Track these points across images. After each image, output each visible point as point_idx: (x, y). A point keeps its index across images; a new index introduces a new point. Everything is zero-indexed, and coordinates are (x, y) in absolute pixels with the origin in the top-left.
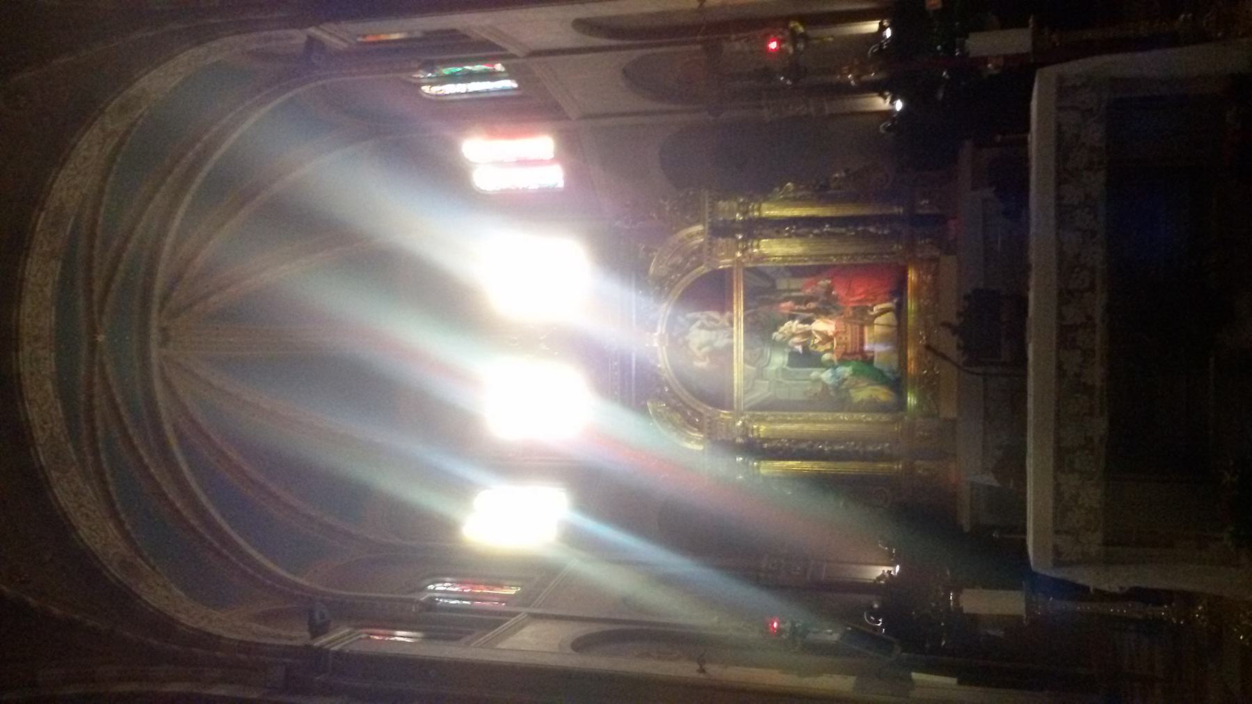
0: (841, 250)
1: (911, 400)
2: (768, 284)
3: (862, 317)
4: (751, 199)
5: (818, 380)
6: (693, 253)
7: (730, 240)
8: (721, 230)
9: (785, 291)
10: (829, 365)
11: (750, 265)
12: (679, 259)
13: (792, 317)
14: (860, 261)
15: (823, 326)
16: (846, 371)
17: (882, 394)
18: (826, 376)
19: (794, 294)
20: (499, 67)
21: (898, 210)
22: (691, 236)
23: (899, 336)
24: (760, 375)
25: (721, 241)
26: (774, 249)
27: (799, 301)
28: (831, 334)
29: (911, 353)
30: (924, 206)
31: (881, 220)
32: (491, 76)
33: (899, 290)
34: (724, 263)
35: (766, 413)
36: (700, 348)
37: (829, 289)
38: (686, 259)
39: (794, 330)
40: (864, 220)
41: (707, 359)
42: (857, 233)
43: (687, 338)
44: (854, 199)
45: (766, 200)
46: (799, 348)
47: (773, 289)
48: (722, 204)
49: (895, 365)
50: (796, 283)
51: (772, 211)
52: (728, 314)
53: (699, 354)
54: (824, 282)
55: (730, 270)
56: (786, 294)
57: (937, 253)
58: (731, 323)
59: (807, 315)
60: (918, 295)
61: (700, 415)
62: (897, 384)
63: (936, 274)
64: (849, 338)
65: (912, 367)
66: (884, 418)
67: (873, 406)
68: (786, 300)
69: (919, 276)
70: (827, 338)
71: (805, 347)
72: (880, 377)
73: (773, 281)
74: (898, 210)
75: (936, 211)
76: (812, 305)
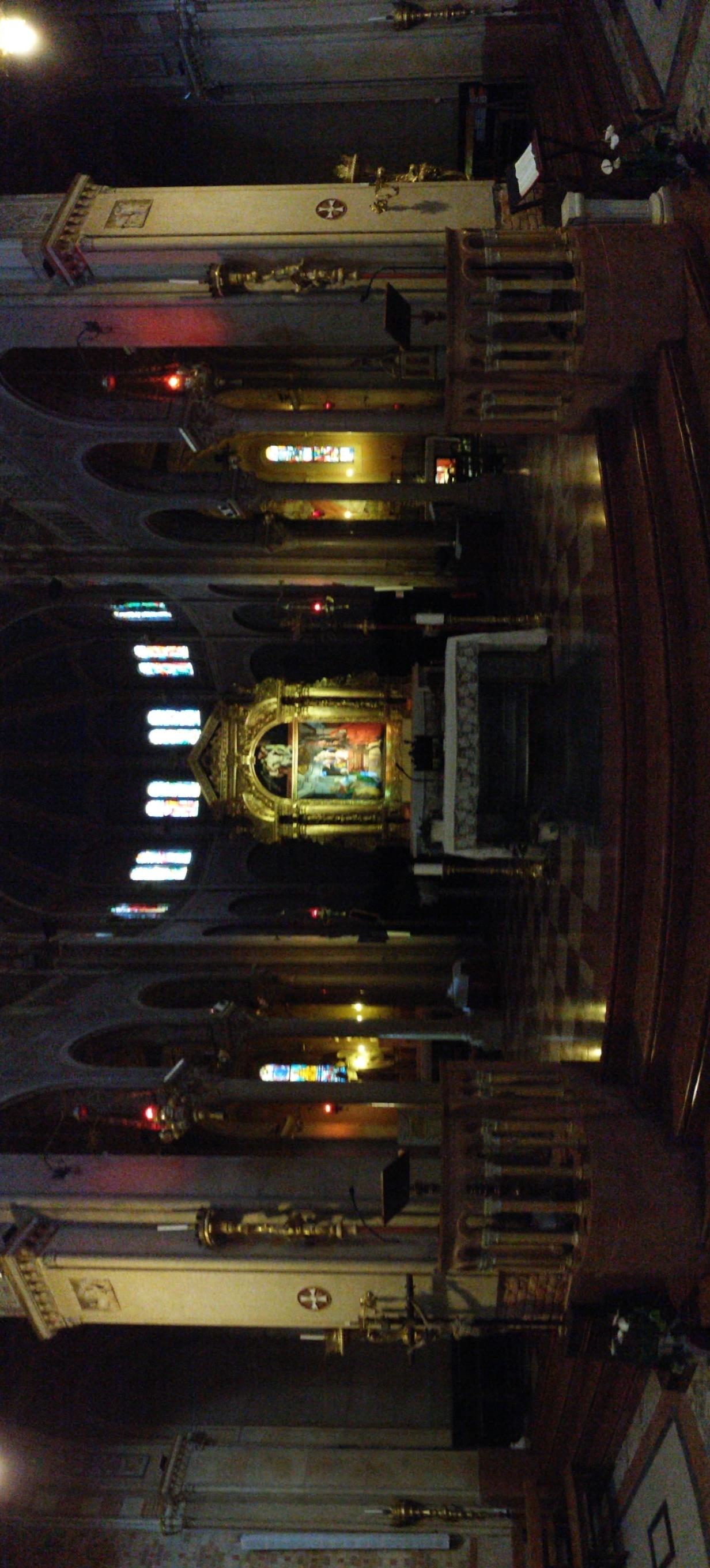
0: (351, 715)
2: (312, 731)
3: (362, 749)
4: (304, 685)
5: (338, 783)
6: (271, 713)
7: (292, 707)
8: (286, 701)
9: (321, 735)
10: (345, 775)
11: (302, 721)
12: (262, 717)
13: (325, 749)
14: (362, 720)
15: (342, 754)
16: (353, 778)
17: (372, 790)
18: (343, 781)
19: (326, 737)
20: (162, 605)
21: (381, 695)
22: (270, 704)
23: (382, 760)
24: (307, 780)
25: (286, 707)
26: (316, 713)
27: (328, 740)
28: (346, 758)
29: (388, 769)
30: (395, 694)
31: (373, 700)
32: (157, 609)
33: (382, 736)
34: (287, 719)
35: (309, 800)
36: (273, 765)
37: (345, 736)
38: (266, 716)
39: (326, 756)
40: (364, 700)
41: (278, 771)
42: (360, 706)
43: (266, 759)
44: (359, 688)
45: (312, 686)
46: (329, 766)
47: (315, 734)
48: (288, 688)
50: (328, 731)
51: (314, 692)
52: (289, 747)
53: (273, 768)
54: (342, 731)
55: (291, 724)
56: (322, 737)
57: (400, 717)
58: (291, 752)
59: (333, 748)
60: (392, 738)
61: (273, 803)
63: (400, 729)
64: (356, 761)
65: (388, 776)
66: (373, 802)
67: (366, 797)
68: (321, 740)
69: (392, 730)
70: (343, 761)
71: (332, 766)
73: (315, 730)
74: (381, 695)
75: (401, 696)
76: (336, 743)
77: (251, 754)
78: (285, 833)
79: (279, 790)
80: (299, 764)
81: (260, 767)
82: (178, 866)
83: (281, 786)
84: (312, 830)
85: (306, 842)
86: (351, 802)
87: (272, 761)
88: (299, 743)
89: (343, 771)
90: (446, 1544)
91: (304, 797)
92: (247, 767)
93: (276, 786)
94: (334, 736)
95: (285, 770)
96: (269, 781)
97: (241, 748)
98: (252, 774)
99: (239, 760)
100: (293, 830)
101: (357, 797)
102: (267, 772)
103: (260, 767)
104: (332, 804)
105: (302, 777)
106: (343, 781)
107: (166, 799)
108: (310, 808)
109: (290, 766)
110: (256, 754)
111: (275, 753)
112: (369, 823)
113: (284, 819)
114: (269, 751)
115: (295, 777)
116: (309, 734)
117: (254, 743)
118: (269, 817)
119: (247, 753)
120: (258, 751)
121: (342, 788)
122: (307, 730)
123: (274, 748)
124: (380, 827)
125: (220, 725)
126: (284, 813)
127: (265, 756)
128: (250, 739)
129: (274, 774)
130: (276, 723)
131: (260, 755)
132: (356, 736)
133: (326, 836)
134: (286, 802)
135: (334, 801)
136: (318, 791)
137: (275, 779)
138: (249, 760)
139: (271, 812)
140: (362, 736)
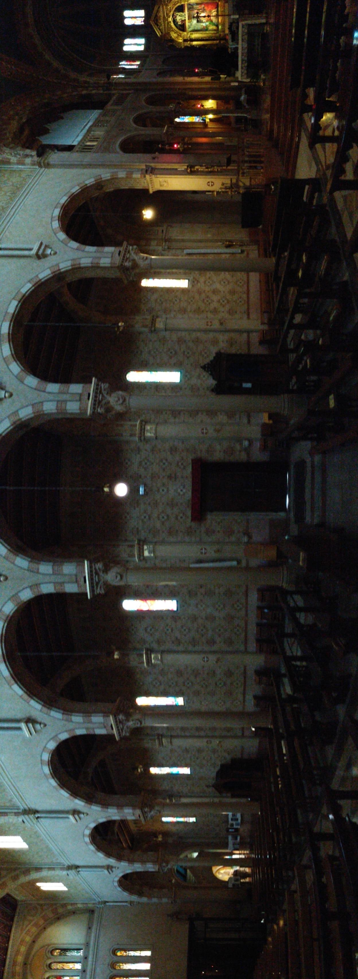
1: (220, 27)
5: (202, 26)
16: (208, 23)
17: (214, 27)
24: (191, 25)
33: (217, 7)
37: (204, 8)
47: (193, 8)
49: (217, 22)
50: (198, 6)
54: (203, 6)
62: (217, 26)
66: (215, 32)
72: (214, 24)
77: (171, 17)
78: (185, 45)
79: (182, 29)
80: (188, 19)
81: (175, 21)
82: (140, 45)
83: (182, 27)
84: (195, 43)
85: (193, 47)
86: (207, 32)
87: (178, 18)
88: (188, 11)
89: (204, 21)
90: (240, 251)
91: (191, 31)
92: (170, 22)
93: (181, 28)
94: (200, 8)
95: (184, 21)
96: (178, 26)
97: (167, 14)
98: (172, 24)
99: (167, 20)
100: (188, 44)
101: (210, 30)
102: (177, 23)
103: (175, 21)
104: (202, 34)
105: (190, 24)
106: (204, 25)
107: (132, 18)
108: (195, 36)
109: (185, 20)
110: (173, 17)
111: (179, 16)
112: (214, 40)
113: (185, 41)
114: (177, 15)
115: (187, 24)
116: (191, 8)
117: (172, 13)
118: (181, 40)
119: (169, 17)
120: (173, 15)
121: (204, 27)
122: (190, 6)
123: (179, 14)
124: (218, 42)
125: (159, 7)
126: (185, 38)
127: (176, 17)
128: (170, 12)
129: (180, 23)
130: (179, 4)
131: (174, 17)
132: (208, 8)
133: (199, 45)
134: (185, 33)
135: (201, 32)
136: (196, 29)
137: (180, 25)
138: (170, 19)
139: (181, 38)
140: (210, 7)
